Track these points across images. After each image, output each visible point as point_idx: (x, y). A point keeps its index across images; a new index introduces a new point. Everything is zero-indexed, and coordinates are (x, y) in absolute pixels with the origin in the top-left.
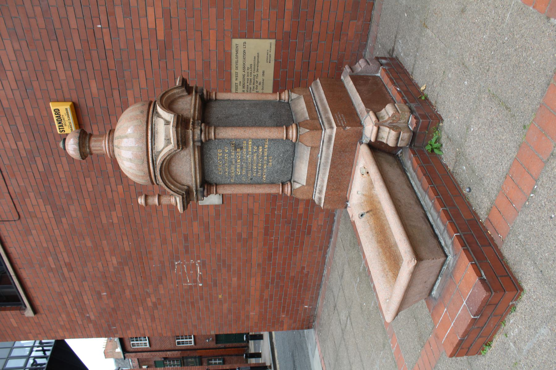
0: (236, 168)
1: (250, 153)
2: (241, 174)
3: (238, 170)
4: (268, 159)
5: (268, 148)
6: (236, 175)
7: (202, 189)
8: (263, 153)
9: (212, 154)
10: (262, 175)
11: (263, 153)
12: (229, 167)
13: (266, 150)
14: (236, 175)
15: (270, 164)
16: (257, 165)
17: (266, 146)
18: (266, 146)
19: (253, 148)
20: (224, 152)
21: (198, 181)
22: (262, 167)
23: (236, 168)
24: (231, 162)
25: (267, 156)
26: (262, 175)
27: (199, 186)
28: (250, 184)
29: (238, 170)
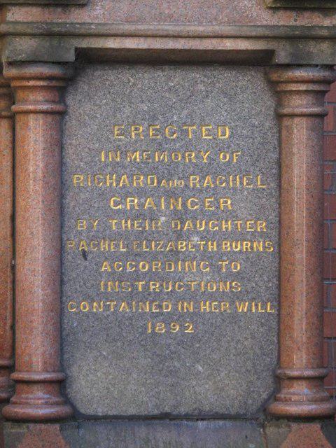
0: (141, 193)
1: (213, 247)
2: (111, 215)
3: (133, 202)
4: (180, 318)
5: (234, 318)
6: (104, 195)
7: (71, 56)
8: (212, 297)
9: (210, 103)
10: (107, 297)
11: (212, 297)
12: (146, 168)
13: (225, 306)
14: (104, 195)
15: (160, 328)
16: (152, 276)
17: (242, 308)
18: (242, 308)
19: (232, 256)
20: (219, 147)
21: (112, 44)
22: (146, 296)
23: (141, 193)
24: (170, 177)
25: (197, 314)
26: (107, 297)
27: (85, 44)
28: (60, 250)
29: (133, 202)
